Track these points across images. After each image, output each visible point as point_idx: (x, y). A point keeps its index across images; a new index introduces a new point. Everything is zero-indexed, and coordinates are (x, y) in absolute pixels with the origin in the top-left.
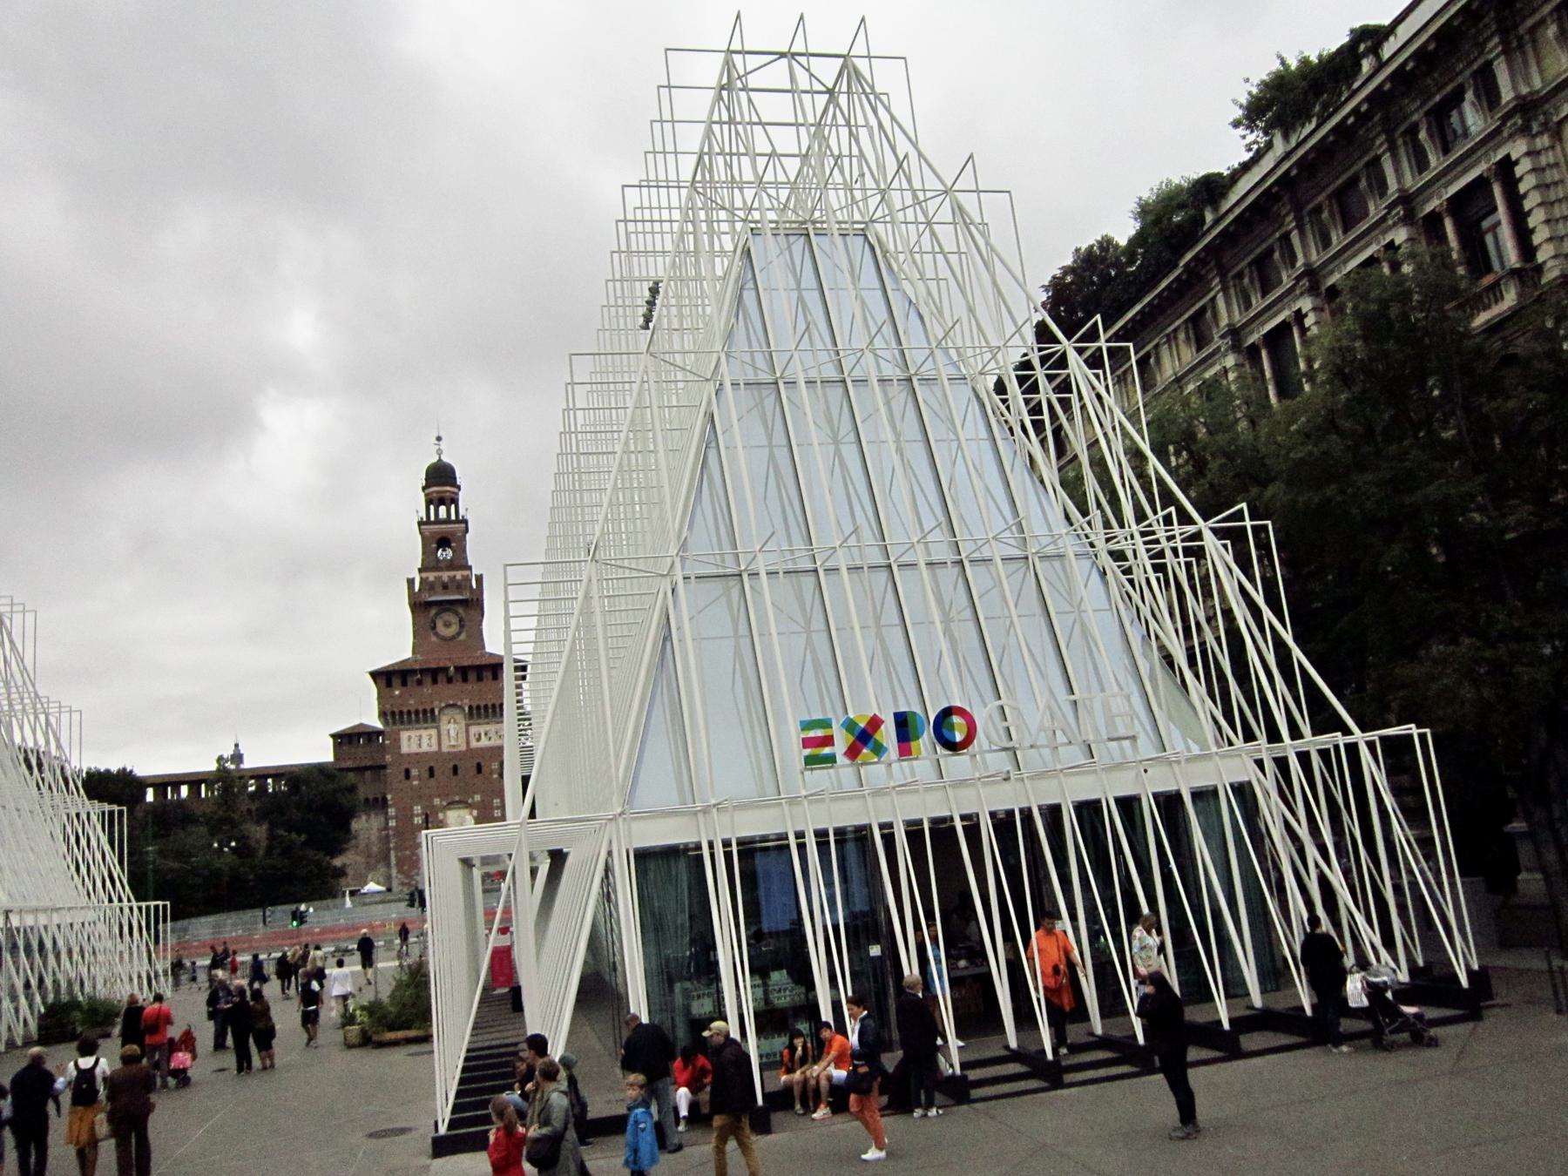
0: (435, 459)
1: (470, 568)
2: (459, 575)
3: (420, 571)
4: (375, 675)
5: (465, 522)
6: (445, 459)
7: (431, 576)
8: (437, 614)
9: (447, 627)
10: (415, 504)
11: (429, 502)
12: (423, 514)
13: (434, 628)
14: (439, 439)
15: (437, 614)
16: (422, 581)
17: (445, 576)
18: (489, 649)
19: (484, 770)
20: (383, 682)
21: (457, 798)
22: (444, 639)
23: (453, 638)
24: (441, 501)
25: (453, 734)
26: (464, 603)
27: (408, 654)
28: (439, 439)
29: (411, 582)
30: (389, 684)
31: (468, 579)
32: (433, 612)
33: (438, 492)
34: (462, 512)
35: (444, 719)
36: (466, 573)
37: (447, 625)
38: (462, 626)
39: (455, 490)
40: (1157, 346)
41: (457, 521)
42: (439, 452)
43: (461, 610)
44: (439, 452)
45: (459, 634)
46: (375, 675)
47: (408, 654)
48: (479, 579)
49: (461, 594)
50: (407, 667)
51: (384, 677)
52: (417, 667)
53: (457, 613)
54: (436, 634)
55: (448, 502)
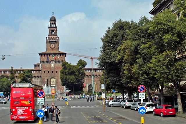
1: (57, 36)
2: (55, 37)
3: (48, 36)
4: (40, 54)
5: (57, 27)
6: (54, 16)
7: (50, 37)
9: (53, 46)
10: (48, 24)
11: (51, 24)
12: (49, 26)
13: (50, 46)
14: (53, 12)
15: (51, 44)
16: (49, 38)
17: (52, 37)
18: (59, 51)
19: (58, 72)
21: (53, 77)
22: (51, 48)
27: (45, 51)
28: (53, 12)
29: (47, 38)
30: (42, 56)
32: (50, 43)
35: (51, 63)
40: (170, 4)
43: (55, 43)
44: (53, 15)
46: (40, 54)
47: (45, 51)
48: (59, 37)
51: (41, 54)
52: (47, 53)
53: (54, 44)
54: (51, 47)
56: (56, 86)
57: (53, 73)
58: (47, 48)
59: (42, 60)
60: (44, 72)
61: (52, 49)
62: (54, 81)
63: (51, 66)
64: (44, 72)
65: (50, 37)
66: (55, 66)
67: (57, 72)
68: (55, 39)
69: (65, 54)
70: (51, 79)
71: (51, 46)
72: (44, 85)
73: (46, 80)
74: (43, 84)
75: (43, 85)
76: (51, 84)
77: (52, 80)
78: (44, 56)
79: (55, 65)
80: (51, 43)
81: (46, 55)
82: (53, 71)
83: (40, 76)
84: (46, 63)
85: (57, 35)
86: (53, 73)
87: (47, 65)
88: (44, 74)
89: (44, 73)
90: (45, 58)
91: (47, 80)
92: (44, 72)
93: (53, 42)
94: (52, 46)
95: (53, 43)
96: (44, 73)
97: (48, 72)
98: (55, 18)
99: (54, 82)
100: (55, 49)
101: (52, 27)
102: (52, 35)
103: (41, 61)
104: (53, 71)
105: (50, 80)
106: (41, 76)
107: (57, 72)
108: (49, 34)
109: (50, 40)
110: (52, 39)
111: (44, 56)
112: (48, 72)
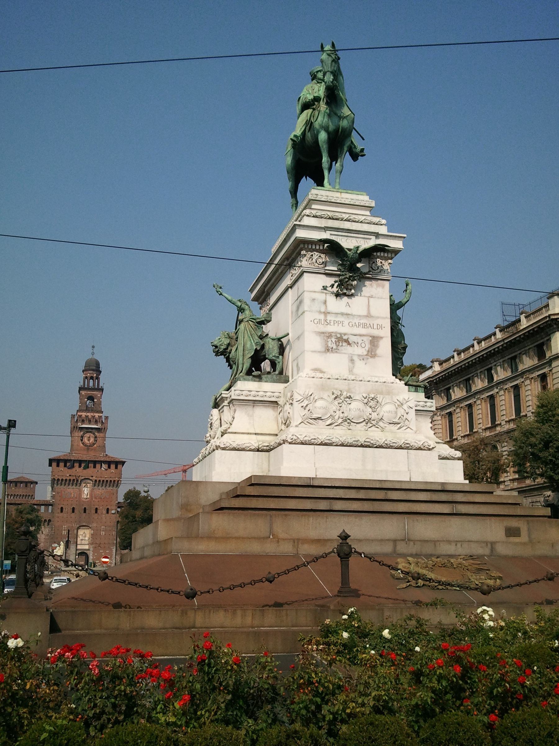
0: (90, 357)
1: (102, 412)
2: (97, 415)
5: (102, 390)
6: (96, 357)
7: (84, 414)
8: (84, 434)
9: (89, 439)
10: (79, 379)
12: (82, 384)
13: (82, 440)
14: (93, 347)
15: (84, 434)
20: (54, 464)
21: (84, 524)
22: (86, 445)
23: (90, 446)
24: (92, 378)
25: (86, 492)
26: (98, 430)
28: (93, 347)
29: (73, 416)
31: (100, 417)
34: (101, 385)
36: (101, 415)
42: (93, 354)
44: (93, 354)
45: (94, 444)
48: (107, 418)
50: (66, 458)
53: (94, 434)
54: (83, 443)
55: (94, 379)
56: (91, 549)
57: (85, 511)
58: (72, 445)
59: (56, 477)
61: (88, 447)
62: (88, 536)
63: (80, 492)
64: (62, 508)
65: (83, 416)
66: (91, 495)
67: (96, 512)
69: (123, 463)
70: (78, 528)
71: (85, 440)
72: (59, 545)
73: (65, 533)
74: (55, 543)
75: (56, 545)
76: (77, 543)
77: (81, 532)
79: (92, 491)
80: (86, 430)
82: (85, 508)
83: (50, 521)
84: (69, 485)
86: (85, 511)
87: (71, 490)
88: (61, 515)
89: (62, 511)
90: (64, 472)
91: (69, 530)
92: (62, 508)
94: (89, 440)
95: (91, 432)
96: (62, 511)
97: (73, 509)
98: (98, 364)
99: (87, 538)
100: (95, 450)
101: (88, 389)
102: (87, 410)
103: (54, 479)
104: (85, 508)
105: (76, 531)
106: (52, 520)
107: (96, 512)
110: (90, 422)
112: (73, 509)
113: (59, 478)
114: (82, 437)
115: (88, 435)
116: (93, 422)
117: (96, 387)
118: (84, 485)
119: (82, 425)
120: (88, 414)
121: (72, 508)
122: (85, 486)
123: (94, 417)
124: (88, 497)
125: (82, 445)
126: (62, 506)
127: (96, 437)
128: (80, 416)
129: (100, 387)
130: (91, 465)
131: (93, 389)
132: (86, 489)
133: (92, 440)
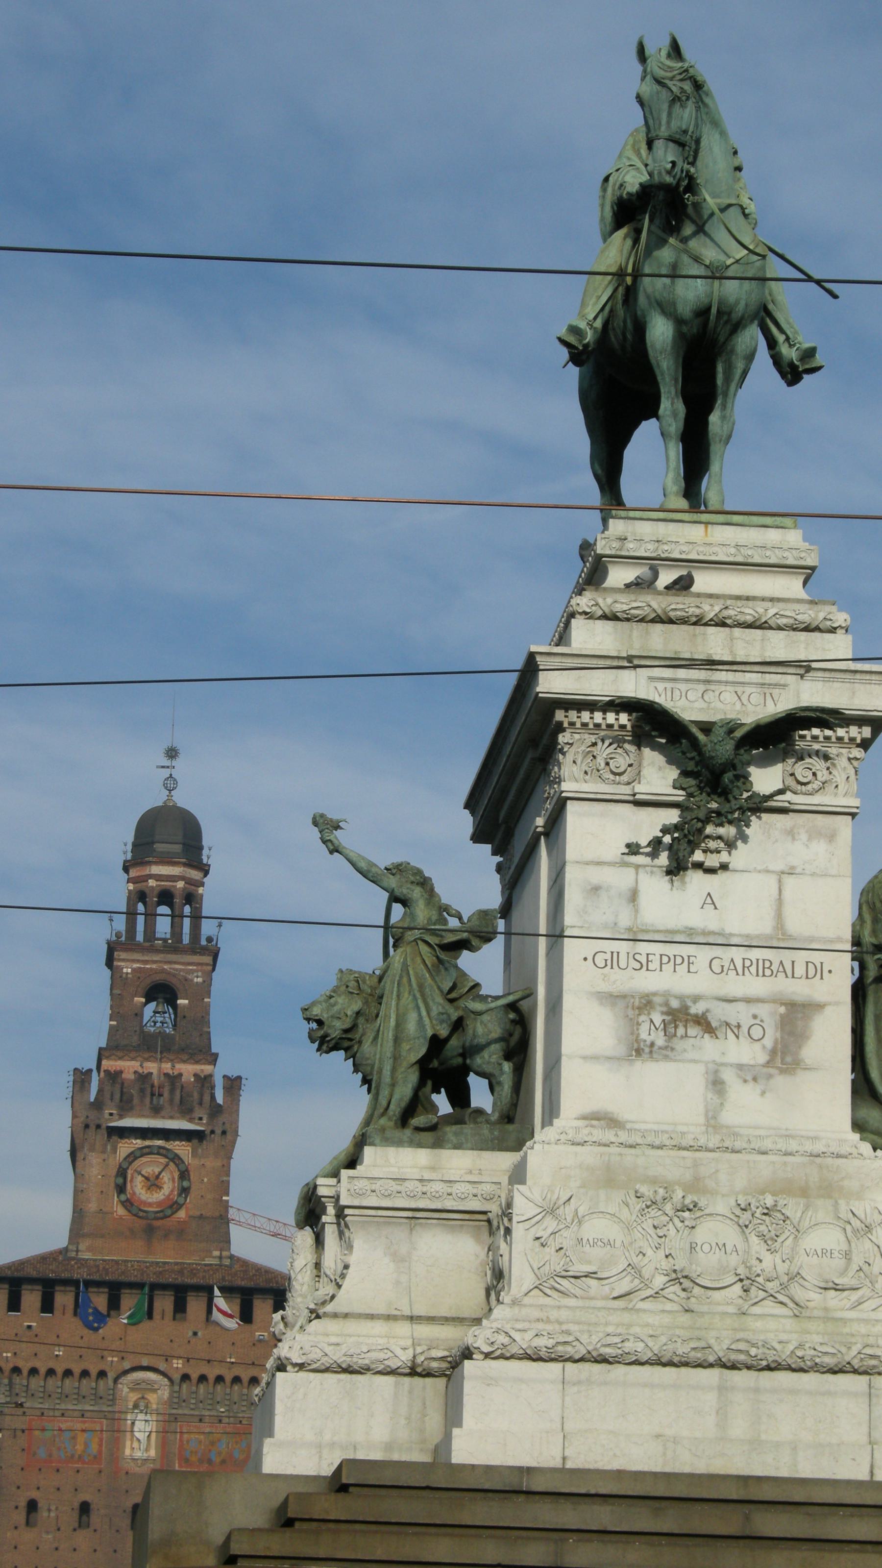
0: (156, 798)
1: (213, 1059)
2: (188, 1070)
3: (101, 1054)
6: (182, 799)
7: (129, 1067)
14: (172, 753)
24: (166, 897)
28: (172, 753)
29: (81, 1078)
31: (205, 1081)
33: (158, 878)
34: (208, 928)
36: (207, 1069)
37: (153, 1183)
38: (185, 1191)
39: (195, 874)
41: (195, 947)
42: (170, 784)
44: (170, 784)
45: (175, 1206)
48: (233, 1085)
49: (191, 1120)
54: (128, 1204)
60: (20, 1517)
64: (32, 1506)
66: (163, 1445)
68: (186, 1111)
71: (138, 1188)
78: (47, 1306)
80: (138, 1143)
81: (63, 1299)
85: (214, 1050)
88: (28, 1536)
92: (32, 1506)
93: (167, 1134)
97: (85, 1508)
100: (181, 1232)
108: (112, 1031)
109: (126, 1107)
111: (47, 1306)
112: (85, 1508)
113: (21, 1364)
114: (122, 1173)
115: (150, 1166)
116: (171, 1101)
117: (186, 939)
118: (133, 1397)
119: (121, 1117)
120: (152, 1067)
121: (76, 1505)
122: (136, 1406)
123: (173, 1080)
124: (152, 1453)
125: (121, 1211)
126: (34, 1494)
127: (184, 1175)
128: (114, 1077)
129: (204, 942)
130: (164, 1303)
131: (174, 946)
132: (141, 1416)
133: (168, 1186)
